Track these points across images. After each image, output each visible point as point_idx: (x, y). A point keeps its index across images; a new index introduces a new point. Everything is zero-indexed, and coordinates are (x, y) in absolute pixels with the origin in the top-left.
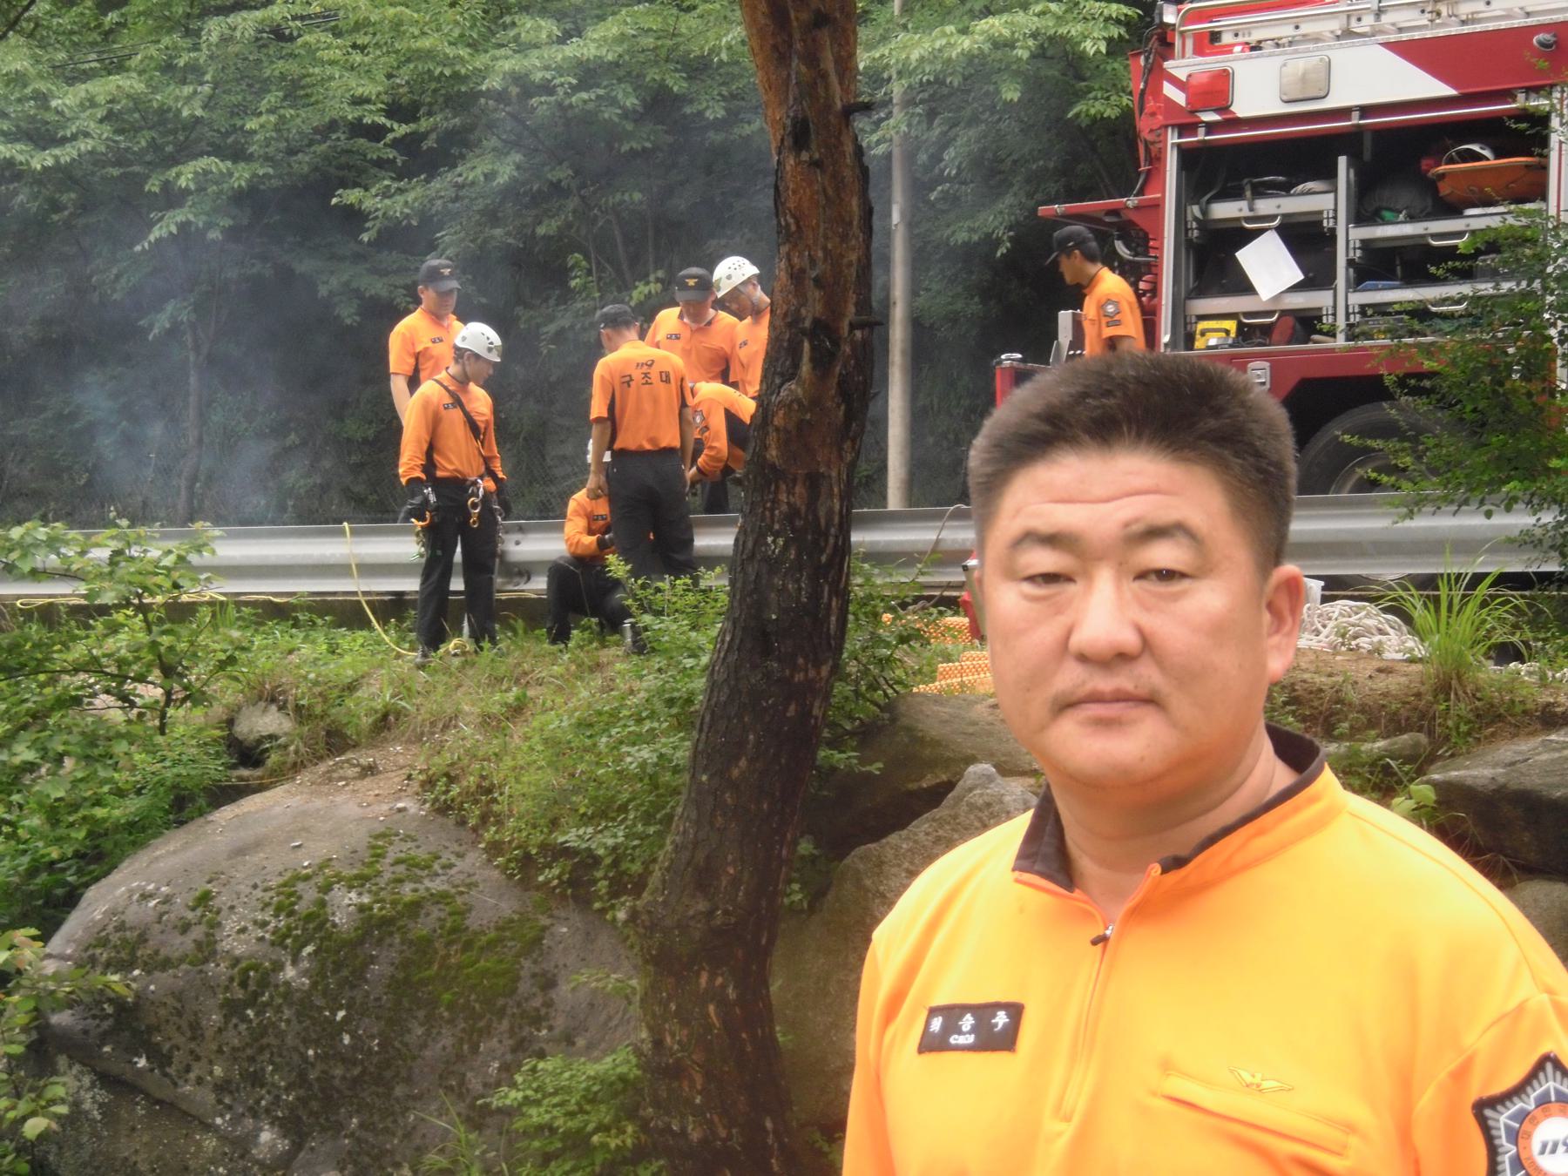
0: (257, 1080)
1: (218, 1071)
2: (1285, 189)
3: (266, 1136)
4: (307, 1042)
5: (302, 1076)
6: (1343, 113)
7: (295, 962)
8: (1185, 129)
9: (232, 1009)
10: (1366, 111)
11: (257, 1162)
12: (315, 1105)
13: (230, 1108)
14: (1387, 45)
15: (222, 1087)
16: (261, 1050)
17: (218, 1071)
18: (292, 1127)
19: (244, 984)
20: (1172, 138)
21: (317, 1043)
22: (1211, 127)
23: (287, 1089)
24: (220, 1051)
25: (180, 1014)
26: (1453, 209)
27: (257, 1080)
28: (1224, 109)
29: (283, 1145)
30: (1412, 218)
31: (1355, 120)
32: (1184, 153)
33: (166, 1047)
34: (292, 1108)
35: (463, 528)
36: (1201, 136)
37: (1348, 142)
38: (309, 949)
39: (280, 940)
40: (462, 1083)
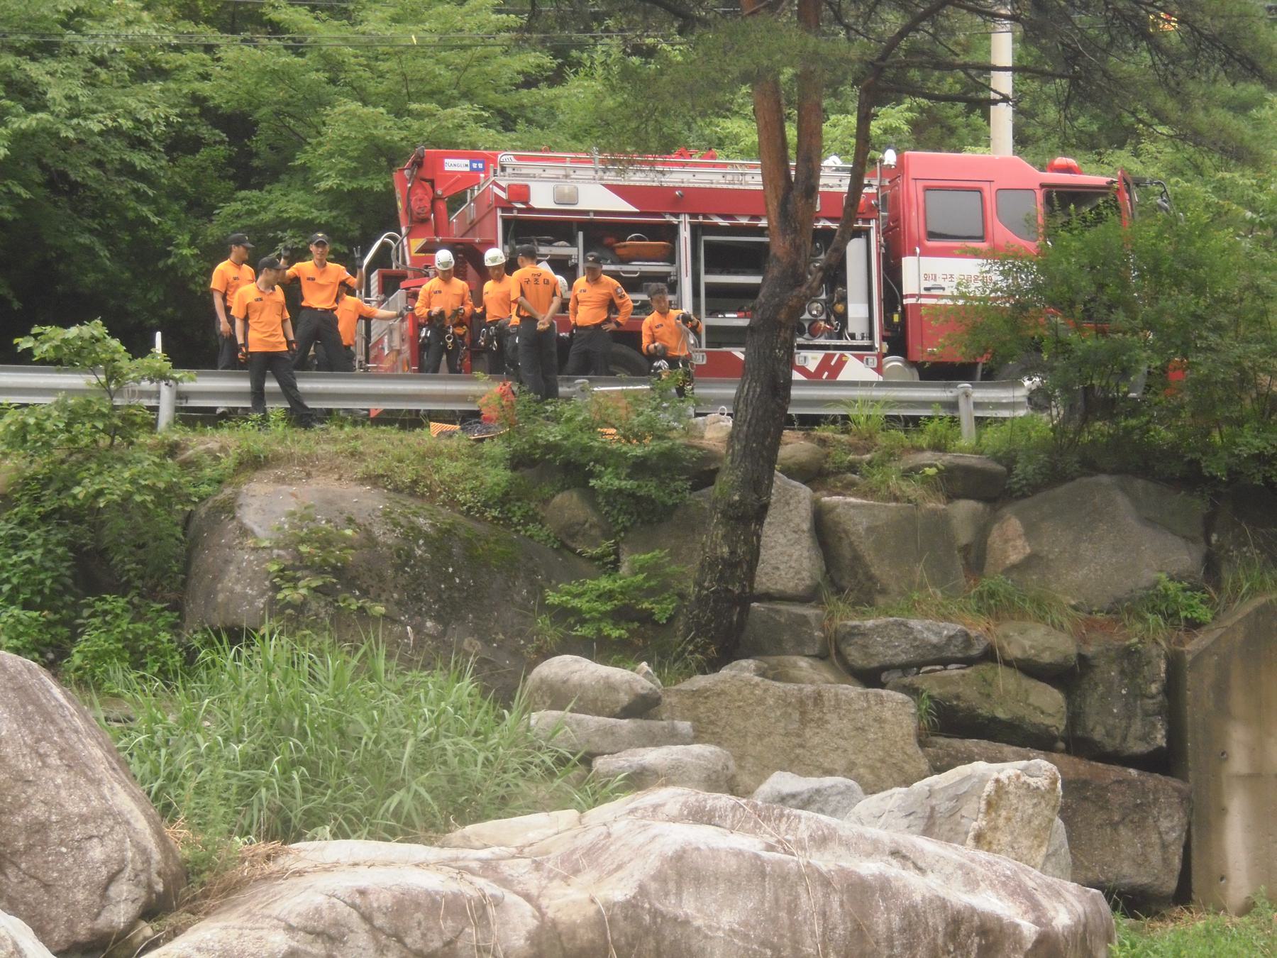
0: (418, 599)
1: (396, 596)
2: (550, 243)
3: (429, 624)
4: (441, 582)
5: (440, 596)
6: (586, 212)
7: (419, 547)
8: (504, 210)
9: (399, 568)
10: (597, 213)
11: (428, 635)
12: (448, 610)
13: (406, 612)
14: (608, 186)
15: (399, 603)
16: (419, 585)
17: (396, 596)
18: (438, 618)
19: (399, 556)
20: (499, 213)
21: (444, 582)
22: (520, 210)
23: (434, 603)
24: (396, 587)
25: (370, 571)
26: (626, 261)
27: (418, 599)
28: (526, 203)
29: (440, 627)
30: (613, 263)
31: (592, 216)
32: (506, 222)
33: (365, 586)
34: (438, 611)
35: (448, 352)
36: (515, 214)
37: (583, 225)
38: (421, 542)
39: (406, 538)
40: (512, 599)
